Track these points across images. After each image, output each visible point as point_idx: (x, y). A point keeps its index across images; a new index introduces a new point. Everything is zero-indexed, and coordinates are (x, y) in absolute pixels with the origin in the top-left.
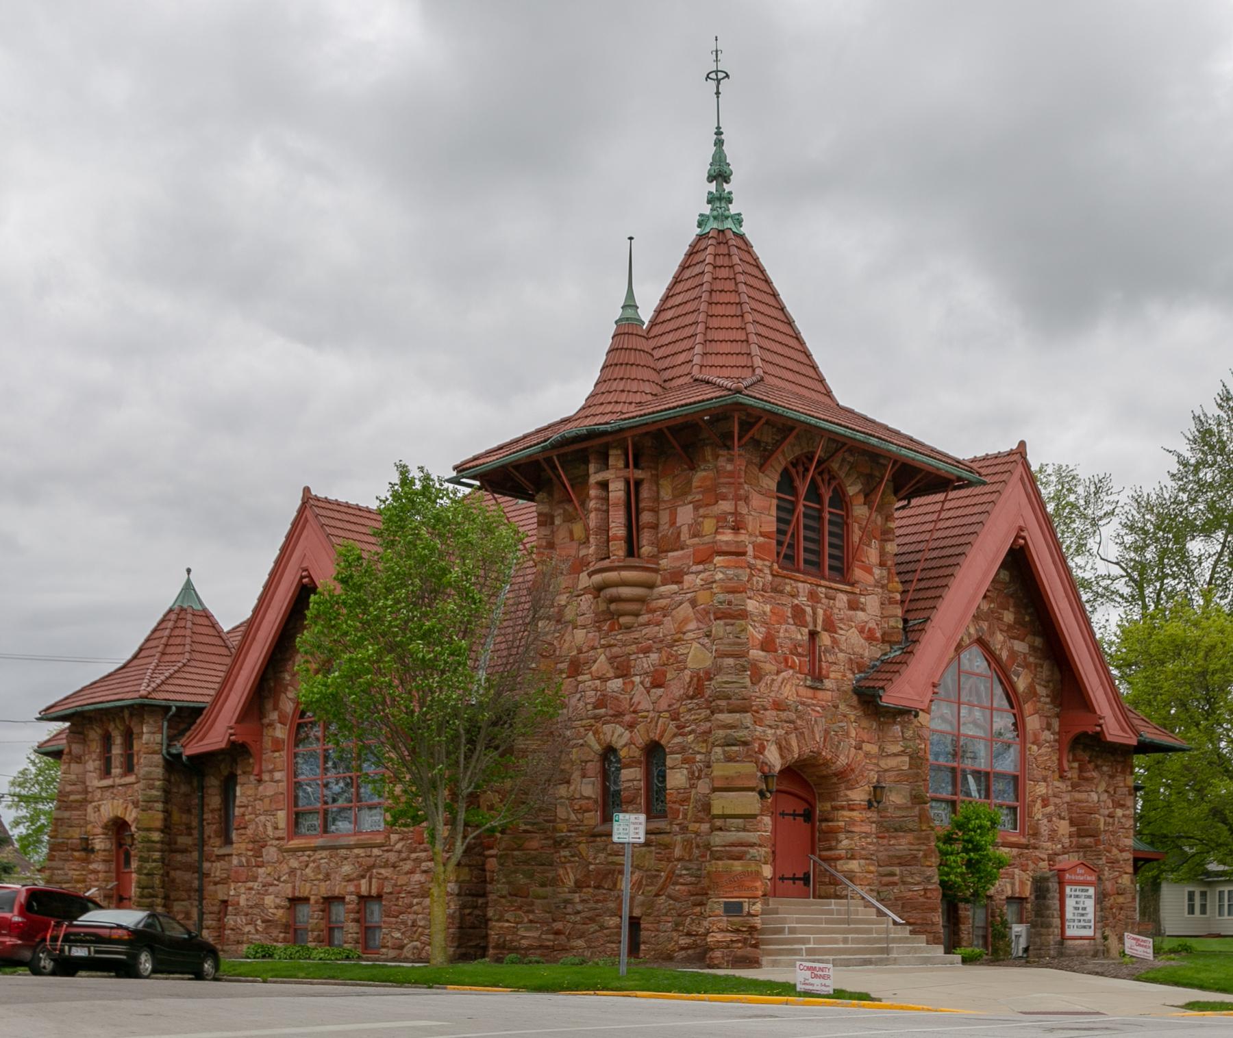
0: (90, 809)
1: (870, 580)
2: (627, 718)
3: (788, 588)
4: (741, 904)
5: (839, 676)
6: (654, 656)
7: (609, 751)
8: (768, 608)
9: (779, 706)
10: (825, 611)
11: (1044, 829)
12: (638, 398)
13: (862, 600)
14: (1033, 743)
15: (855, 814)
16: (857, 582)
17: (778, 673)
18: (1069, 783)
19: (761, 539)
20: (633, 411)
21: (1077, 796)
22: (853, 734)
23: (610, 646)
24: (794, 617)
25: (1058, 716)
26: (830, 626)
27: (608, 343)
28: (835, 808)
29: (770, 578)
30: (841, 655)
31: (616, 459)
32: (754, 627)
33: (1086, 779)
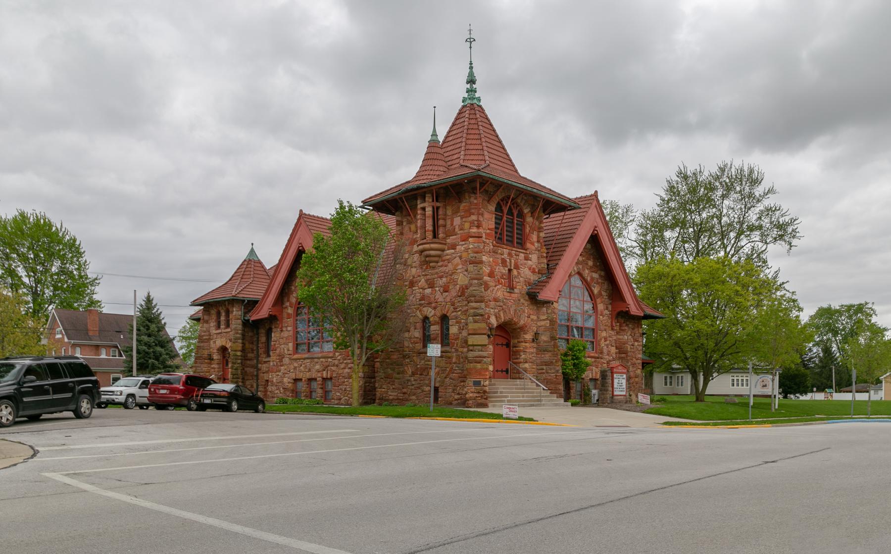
1: (533, 248)
2: (433, 305)
6: (444, 279)
7: (426, 318)
9: (496, 300)
11: (605, 350)
12: (438, 173)
20: (435, 178)
26: (517, 267)
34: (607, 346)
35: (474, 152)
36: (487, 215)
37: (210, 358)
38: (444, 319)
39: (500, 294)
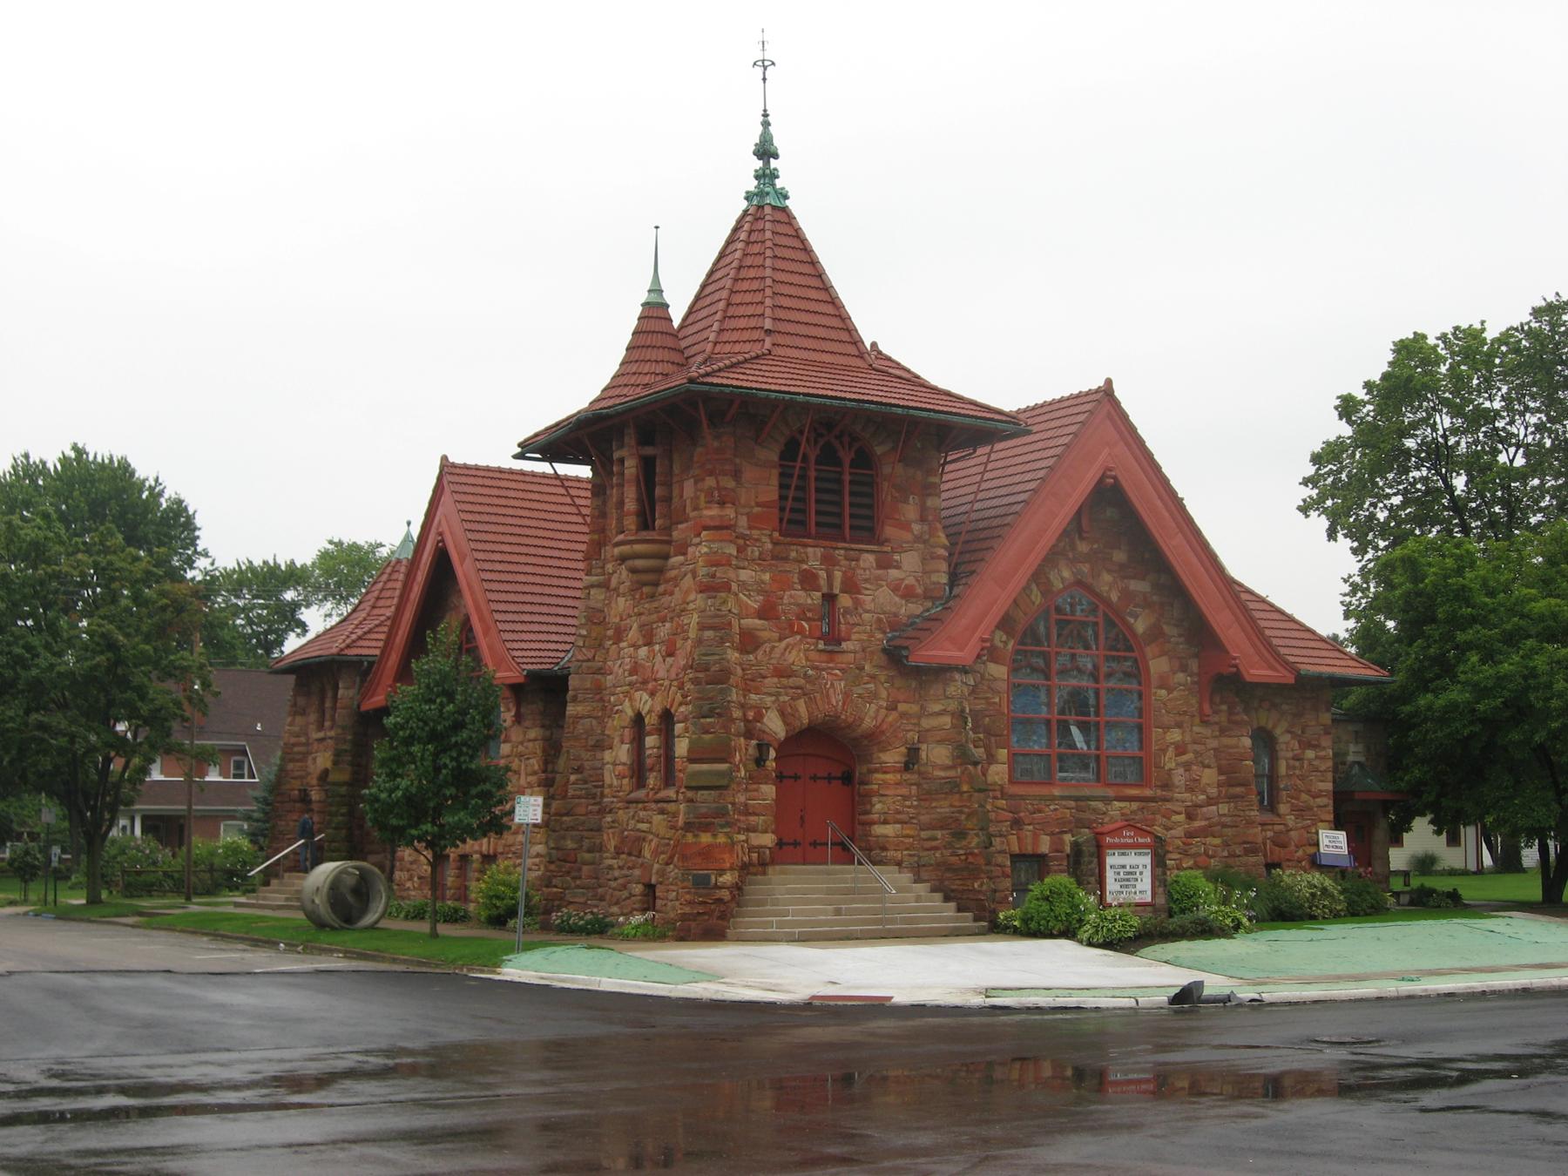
0: (310, 762)
1: (909, 537)
2: (650, 686)
3: (793, 554)
4: (708, 876)
5: (864, 637)
6: (668, 625)
8: (767, 577)
9: (782, 672)
10: (844, 573)
11: (1179, 777)
12: (646, 380)
13: (896, 557)
14: (1160, 687)
15: (888, 776)
16: (887, 540)
17: (780, 640)
18: (1217, 728)
19: (757, 510)
21: (1226, 741)
22: (884, 694)
23: (641, 614)
24: (802, 582)
25: (1196, 656)
26: (851, 587)
27: (633, 323)
28: (871, 771)
29: (770, 546)
30: (866, 616)
31: (630, 439)
32: (749, 596)
33: (1236, 723)
34: (1187, 766)
35: (742, 323)
36: (749, 473)
37: (304, 798)
38: (667, 717)
39: (796, 658)
